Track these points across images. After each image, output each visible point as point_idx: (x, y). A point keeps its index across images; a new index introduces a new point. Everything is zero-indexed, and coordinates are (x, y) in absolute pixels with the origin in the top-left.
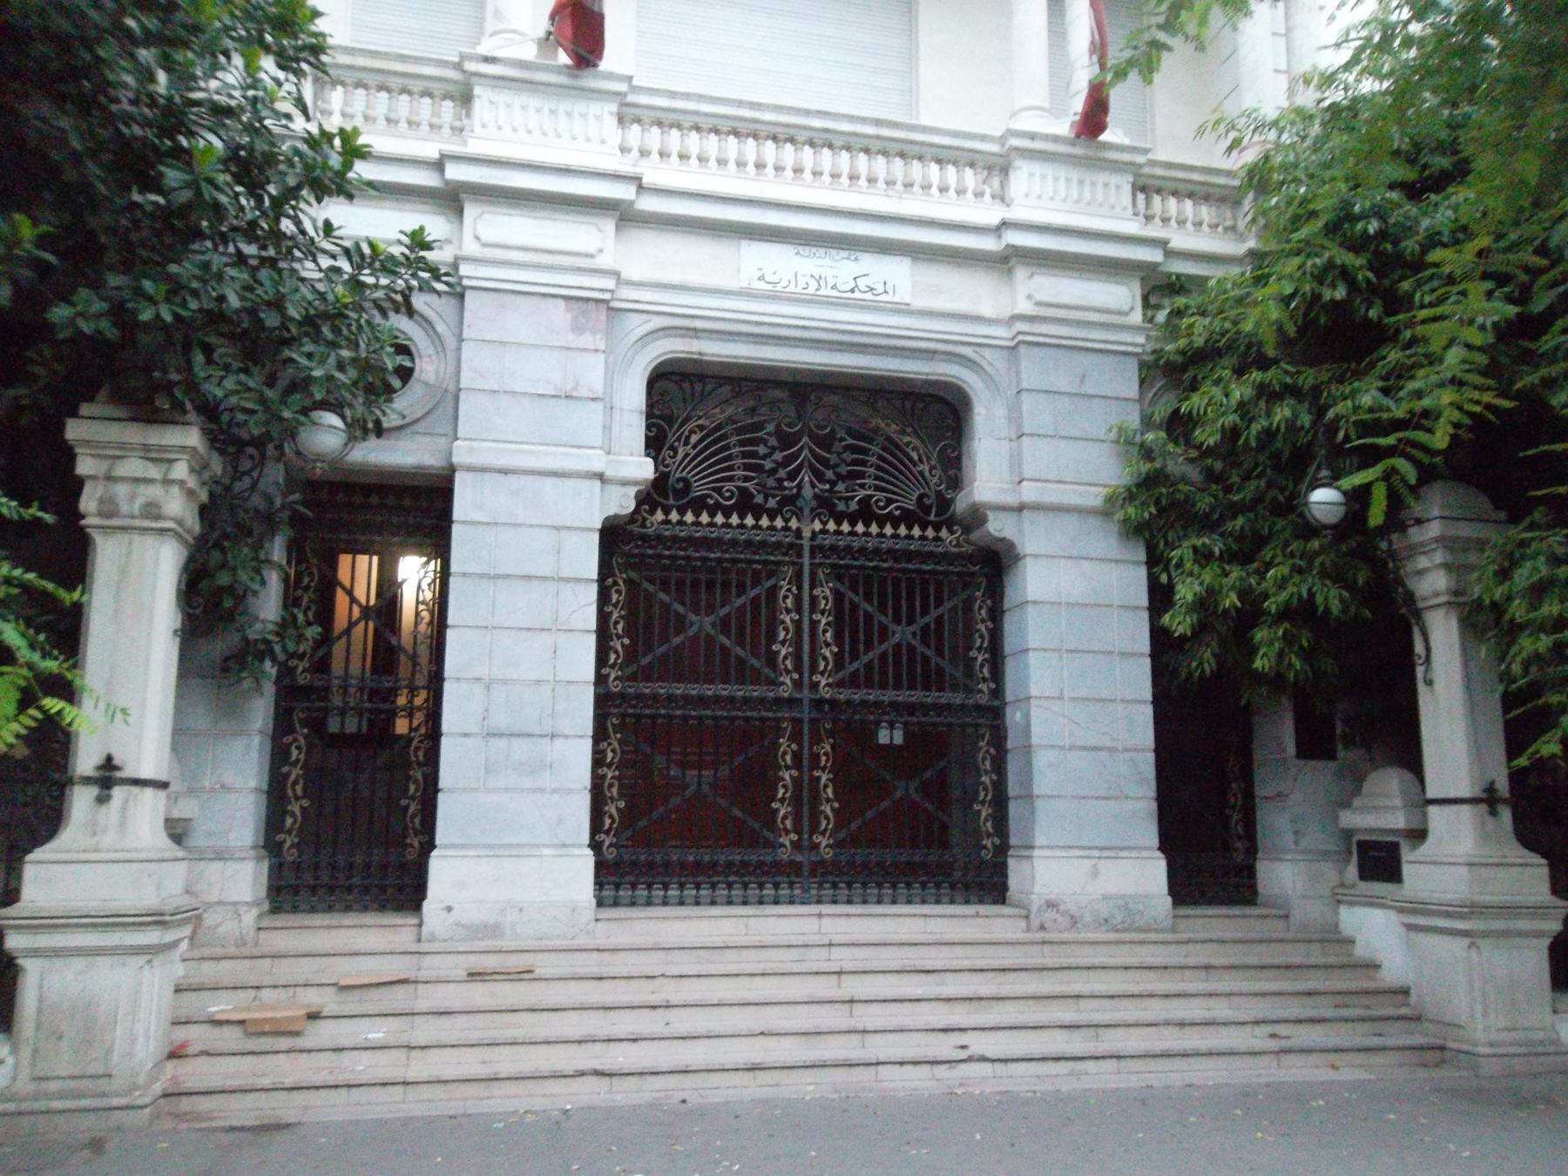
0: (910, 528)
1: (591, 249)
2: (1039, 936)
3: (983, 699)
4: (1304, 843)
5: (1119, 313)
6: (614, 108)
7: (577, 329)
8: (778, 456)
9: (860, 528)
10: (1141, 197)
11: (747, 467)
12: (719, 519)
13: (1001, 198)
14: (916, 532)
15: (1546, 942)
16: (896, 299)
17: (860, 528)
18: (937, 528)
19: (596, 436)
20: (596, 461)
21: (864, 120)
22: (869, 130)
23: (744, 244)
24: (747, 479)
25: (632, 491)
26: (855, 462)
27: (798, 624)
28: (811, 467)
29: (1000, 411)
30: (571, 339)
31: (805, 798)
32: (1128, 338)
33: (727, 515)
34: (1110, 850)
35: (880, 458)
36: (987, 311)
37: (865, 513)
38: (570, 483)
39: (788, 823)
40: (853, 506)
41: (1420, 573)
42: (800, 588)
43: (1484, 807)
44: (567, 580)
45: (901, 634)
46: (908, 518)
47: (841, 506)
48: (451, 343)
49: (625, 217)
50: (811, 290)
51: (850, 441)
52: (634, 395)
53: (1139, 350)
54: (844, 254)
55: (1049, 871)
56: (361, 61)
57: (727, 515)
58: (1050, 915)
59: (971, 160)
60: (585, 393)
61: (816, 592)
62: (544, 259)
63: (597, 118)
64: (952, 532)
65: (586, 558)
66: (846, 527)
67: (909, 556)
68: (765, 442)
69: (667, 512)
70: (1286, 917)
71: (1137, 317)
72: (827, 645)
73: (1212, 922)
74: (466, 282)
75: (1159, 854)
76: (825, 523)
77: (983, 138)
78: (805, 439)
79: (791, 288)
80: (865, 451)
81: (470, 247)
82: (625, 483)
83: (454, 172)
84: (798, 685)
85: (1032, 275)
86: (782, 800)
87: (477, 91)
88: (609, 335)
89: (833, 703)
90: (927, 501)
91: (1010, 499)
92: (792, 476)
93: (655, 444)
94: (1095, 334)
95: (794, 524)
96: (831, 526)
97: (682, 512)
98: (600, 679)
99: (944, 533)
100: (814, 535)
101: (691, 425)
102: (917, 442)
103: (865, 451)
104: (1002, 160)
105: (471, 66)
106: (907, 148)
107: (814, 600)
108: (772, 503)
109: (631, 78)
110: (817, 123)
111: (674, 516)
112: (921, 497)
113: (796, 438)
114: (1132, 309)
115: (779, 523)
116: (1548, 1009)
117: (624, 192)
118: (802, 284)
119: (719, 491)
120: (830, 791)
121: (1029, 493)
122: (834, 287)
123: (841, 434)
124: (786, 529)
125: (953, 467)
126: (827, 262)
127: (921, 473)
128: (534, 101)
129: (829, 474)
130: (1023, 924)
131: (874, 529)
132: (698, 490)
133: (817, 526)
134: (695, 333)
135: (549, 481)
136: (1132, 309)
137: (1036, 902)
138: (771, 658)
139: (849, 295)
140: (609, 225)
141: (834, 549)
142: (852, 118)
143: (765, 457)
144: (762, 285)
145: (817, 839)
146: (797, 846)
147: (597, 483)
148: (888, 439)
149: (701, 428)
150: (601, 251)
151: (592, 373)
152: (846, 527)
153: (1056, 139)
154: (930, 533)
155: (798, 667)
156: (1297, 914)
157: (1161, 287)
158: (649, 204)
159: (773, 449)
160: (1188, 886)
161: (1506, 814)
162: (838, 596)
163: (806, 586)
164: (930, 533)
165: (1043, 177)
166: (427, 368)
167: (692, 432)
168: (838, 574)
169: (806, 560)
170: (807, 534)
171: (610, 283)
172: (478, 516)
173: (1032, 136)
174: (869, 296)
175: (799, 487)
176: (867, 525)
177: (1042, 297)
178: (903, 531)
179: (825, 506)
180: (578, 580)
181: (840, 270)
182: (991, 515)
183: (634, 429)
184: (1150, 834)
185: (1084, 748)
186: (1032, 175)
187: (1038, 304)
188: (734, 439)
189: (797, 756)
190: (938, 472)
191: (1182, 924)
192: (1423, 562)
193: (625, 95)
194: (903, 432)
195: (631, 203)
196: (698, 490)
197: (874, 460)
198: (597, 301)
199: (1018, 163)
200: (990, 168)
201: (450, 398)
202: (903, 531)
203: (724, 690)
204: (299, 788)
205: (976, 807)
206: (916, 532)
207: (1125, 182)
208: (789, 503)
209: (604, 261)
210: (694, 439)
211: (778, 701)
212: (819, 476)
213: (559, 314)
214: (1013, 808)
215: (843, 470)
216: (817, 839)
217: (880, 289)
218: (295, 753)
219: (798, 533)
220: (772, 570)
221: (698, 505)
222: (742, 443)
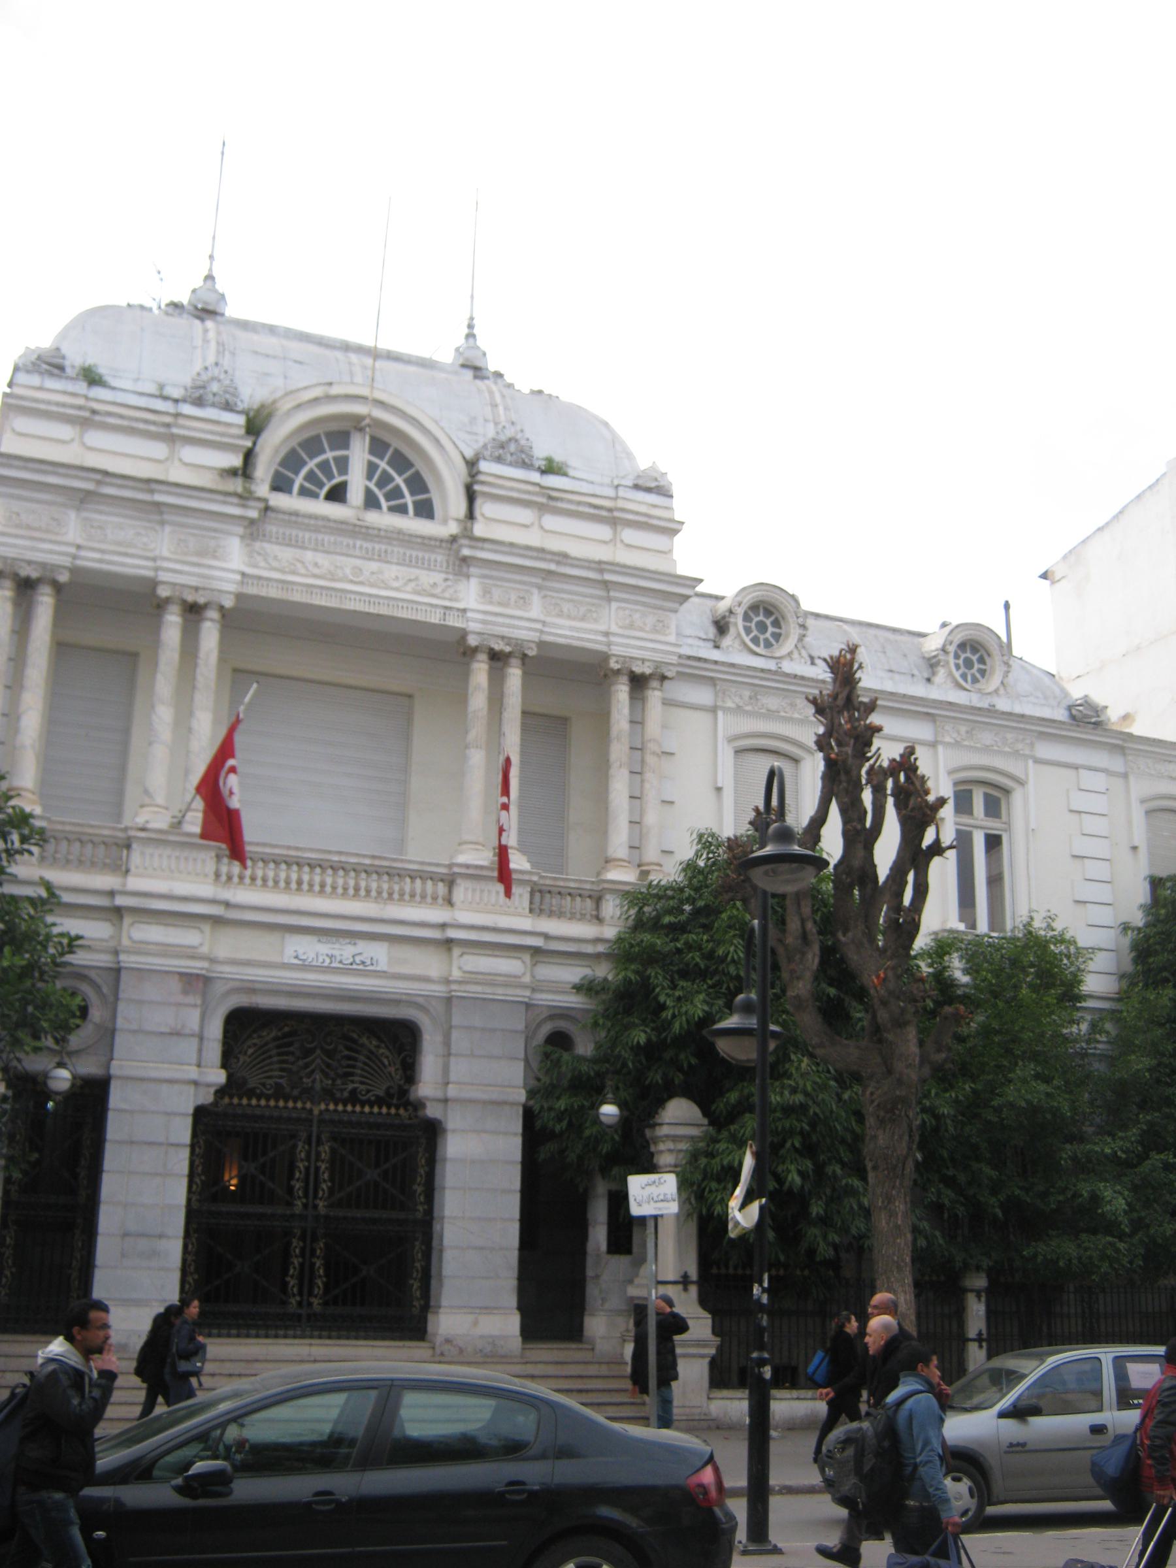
0: (380, 1108)
2: (437, 1359)
3: (419, 1215)
4: (607, 1306)
5: (515, 977)
6: (213, 854)
7: (185, 992)
8: (301, 1063)
9: (349, 1108)
11: (282, 1070)
12: (263, 1102)
13: (449, 902)
14: (384, 1110)
15: (707, 1360)
16: (378, 969)
17: (349, 1108)
18: (397, 1108)
19: (194, 1058)
20: (193, 1073)
21: (364, 856)
22: (367, 861)
23: (287, 936)
24: (281, 1077)
25: (212, 1090)
26: (349, 1066)
27: (307, 1169)
28: (322, 1071)
29: (439, 1038)
30: (180, 998)
31: (306, 1277)
33: (268, 1100)
34: (487, 1310)
35: (365, 1063)
37: (354, 1098)
38: (176, 1087)
39: (295, 1290)
40: (346, 1094)
41: (661, 1152)
42: (310, 1144)
43: (680, 1287)
44: (172, 1145)
45: (372, 1174)
46: (380, 1102)
47: (338, 1095)
48: (111, 999)
50: (326, 964)
51: (346, 1053)
52: (215, 1030)
54: (348, 941)
55: (449, 1321)
57: (268, 1100)
58: (446, 1347)
59: (433, 877)
60: (187, 1031)
61: (321, 1149)
62: (166, 950)
64: (406, 1110)
65: (183, 1131)
66: (340, 1108)
67: (378, 1126)
68: (292, 1053)
69: (231, 1097)
70: (593, 1349)
72: (325, 1181)
73: (546, 1352)
74: (122, 965)
75: (517, 1312)
76: (327, 1105)
77: (437, 865)
78: (318, 1051)
79: (314, 963)
80: (355, 1059)
82: (208, 1085)
83: (120, 901)
84: (305, 1206)
86: (292, 1277)
87: (134, 846)
88: (204, 995)
89: (327, 1217)
90: (392, 1091)
91: (439, 1094)
92: (309, 1075)
93: (227, 1059)
94: (500, 990)
95: (308, 1105)
96: (332, 1107)
97: (240, 1098)
98: (189, 1200)
99: (402, 1111)
100: (321, 1112)
101: (250, 1042)
102: (388, 1053)
103: (355, 1059)
105: (132, 833)
106: (391, 871)
107: (318, 1154)
108: (296, 1092)
110: (336, 858)
111: (236, 1101)
112: (389, 1088)
113: (312, 1051)
114: (524, 974)
115: (299, 1105)
116: (705, 1396)
118: (321, 960)
119: (264, 1085)
120: (321, 1271)
121: (452, 1091)
123: (341, 1047)
124: (304, 1108)
125: (410, 1070)
126: (337, 946)
127: (390, 1074)
128: (168, 851)
129: (332, 1074)
130: (430, 1352)
131: (358, 1109)
132: (252, 1083)
133: (323, 1107)
134: (253, 991)
135: (165, 1087)
136: (524, 974)
137: (439, 1340)
138: (290, 1190)
140: (207, 928)
141: (332, 1121)
142: (357, 855)
143: (293, 1063)
144: (296, 961)
145: (313, 1300)
146: (300, 1304)
147: (192, 1089)
148: (371, 1052)
149: (255, 1045)
151: (193, 1019)
152: (340, 1108)
153: (482, 867)
154: (393, 1111)
155: (306, 1195)
156: (598, 1347)
159: (298, 1058)
160: (529, 1333)
161: (693, 1290)
162: (333, 1151)
163: (314, 1144)
164: (393, 1111)
165: (474, 890)
166: (96, 1014)
167: (249, 1047)
168: (334, 1138)
169: (315, 1129)
170: (316, 1112)
171: (205, 964)
172: (123, 1106)
174: (361, 967)
175: (314, 1081)
176: (354, 1106)
177: (468, 968)
178: (376, 1110)
179: (329, 1094)
180: (178, 1145)
181: (345, 951)
182: (428, 1104)
183: (214, 1051)
184: (512, 1300)
185: (475, 1248)
186: (466, 889)
187: (465, 972)
188: (274, 1052)
189: (303, 1250)
190: (400, 1072)
191: (528, 1353)
192: (662, 1147)
194: (378, 1047)
196: (252, 1083)
197: (360, 1064)
198: (198, 975)
199: (459, 881)
201: (109, 1033)
202: (376, 1110)
203: (260, 1209)
204: (10, 1262)
205: (411, 1282)
206: (384, 1110)
208: (307, 1093)
209: (205, 950)
210: (250, 1051)
211: (293, 1216)
212: (326, 1076)
213: (175, 985)
214: (434, 1283)
215: (340, 1071)
216: (313, 1300)
217: (369, 962)
218: (8, 1240)
219: (311, 1111)
220: (293, 1136)
221: (251, 1093)
222: (279, 1054)
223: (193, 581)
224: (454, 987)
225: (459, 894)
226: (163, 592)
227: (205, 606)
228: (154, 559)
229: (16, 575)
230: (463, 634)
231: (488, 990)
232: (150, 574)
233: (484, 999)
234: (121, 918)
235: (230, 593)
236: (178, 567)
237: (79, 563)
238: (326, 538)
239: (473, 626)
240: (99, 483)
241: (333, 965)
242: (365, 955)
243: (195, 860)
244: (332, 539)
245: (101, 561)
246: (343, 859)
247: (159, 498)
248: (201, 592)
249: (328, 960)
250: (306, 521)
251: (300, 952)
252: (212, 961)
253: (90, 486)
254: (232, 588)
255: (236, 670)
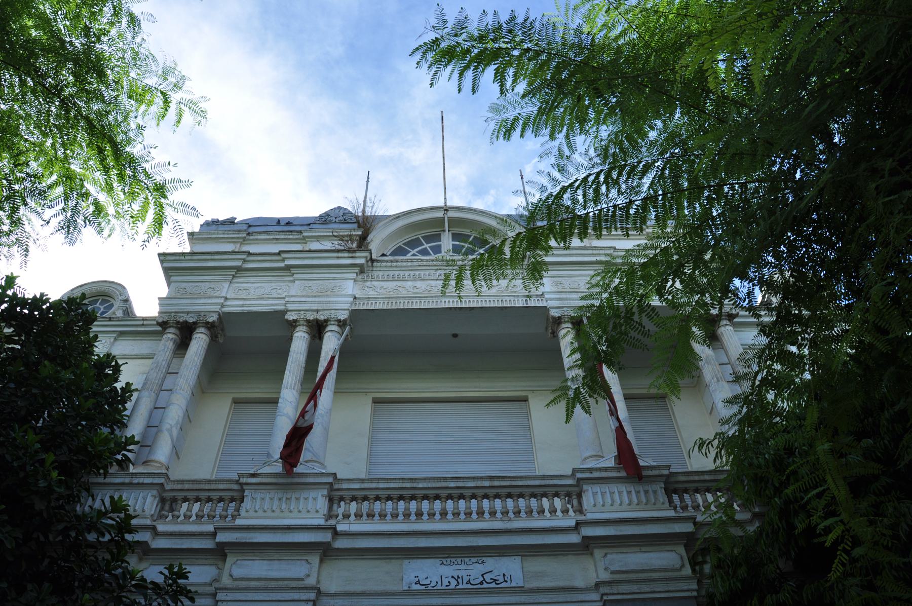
1: (302, 575)
5: (673, 570)
6: (325, 492)
10: (675, 497)
13: (580, 510)
16: (513, 584)
22: (487, 484)
32: (683, 585)
36: (579, 583)
49: (326, 552)
50: (452, 586)
53: (695, 594)
56: (187, 486)
63: (315, 499)
71: (688, 571)
77: (561, 477)
81: (226, 581)
83: (222, 537)
85: (605, 555)
94: (660, 587)
104: (576, 489)
109: (335, 474)
114: (683, 566)
117: (326, 537)
118: (445, 582)
122: (469, 582)
126: (463, 567)
136: (683, 566)
139: (479, 586)
144: (418, 587)
150: (308, 576)
153: (606, 469)
157: (697, 547)
158: (340, 543)
173: (591, 470)
174: (493, 585)
186: (595, 494)
187: (613, 573)
193: (331, 484)
195: (328, 544)
199: (585, 487)
200: (569, 495)
207: (659, 487)
209: (311, 581)
217: (501, 579)
223: (315, 307)
224: (604, 590)
225: (588, 500)
226: (290, 317)
227: (326, 321)
228: (284, 298)
229: (178, 322)
230: (545, 309)
231: (645, 588)
232: (282, 308)
233: (644, 600)
234: (224, 557)
235: (344, 310)
236: (303, 299)
237: (226, 309)
238: (422, 273)
239: (551, 304)
240: (245, 261)
241: (460, 586)
242: (496, 572)
243: (306, 499)
244: (427, 272)
245: (243, 306)
246: (460, 484)
247: (287, 262)
248: (320, 313)
249: (454, 583)
250: (405, 264)
251: (422, 577)
252: (319, 592)
253: (239, 263)
254: (347, 306)
255: (376, 401)
